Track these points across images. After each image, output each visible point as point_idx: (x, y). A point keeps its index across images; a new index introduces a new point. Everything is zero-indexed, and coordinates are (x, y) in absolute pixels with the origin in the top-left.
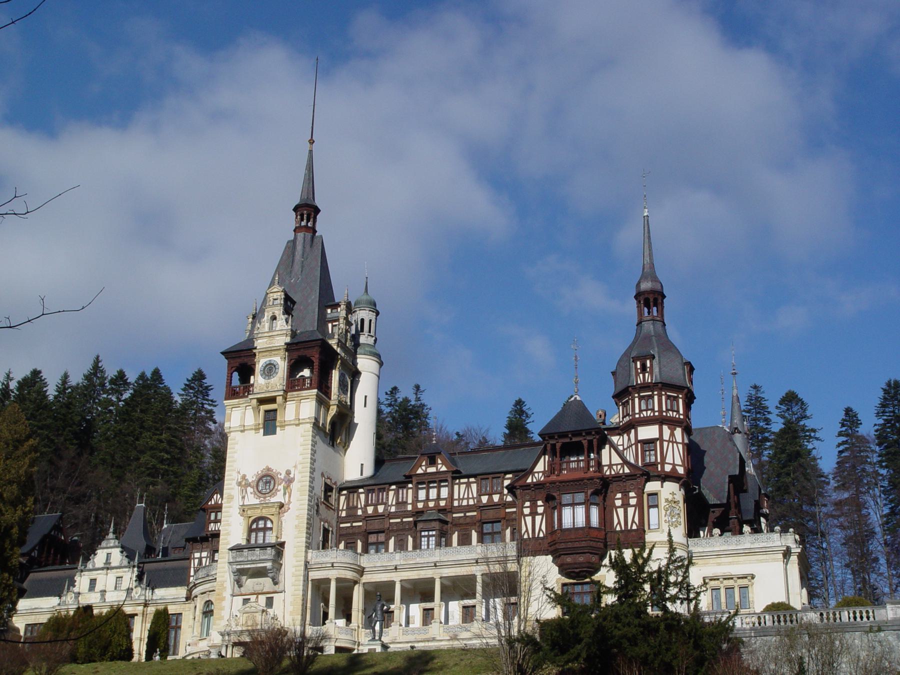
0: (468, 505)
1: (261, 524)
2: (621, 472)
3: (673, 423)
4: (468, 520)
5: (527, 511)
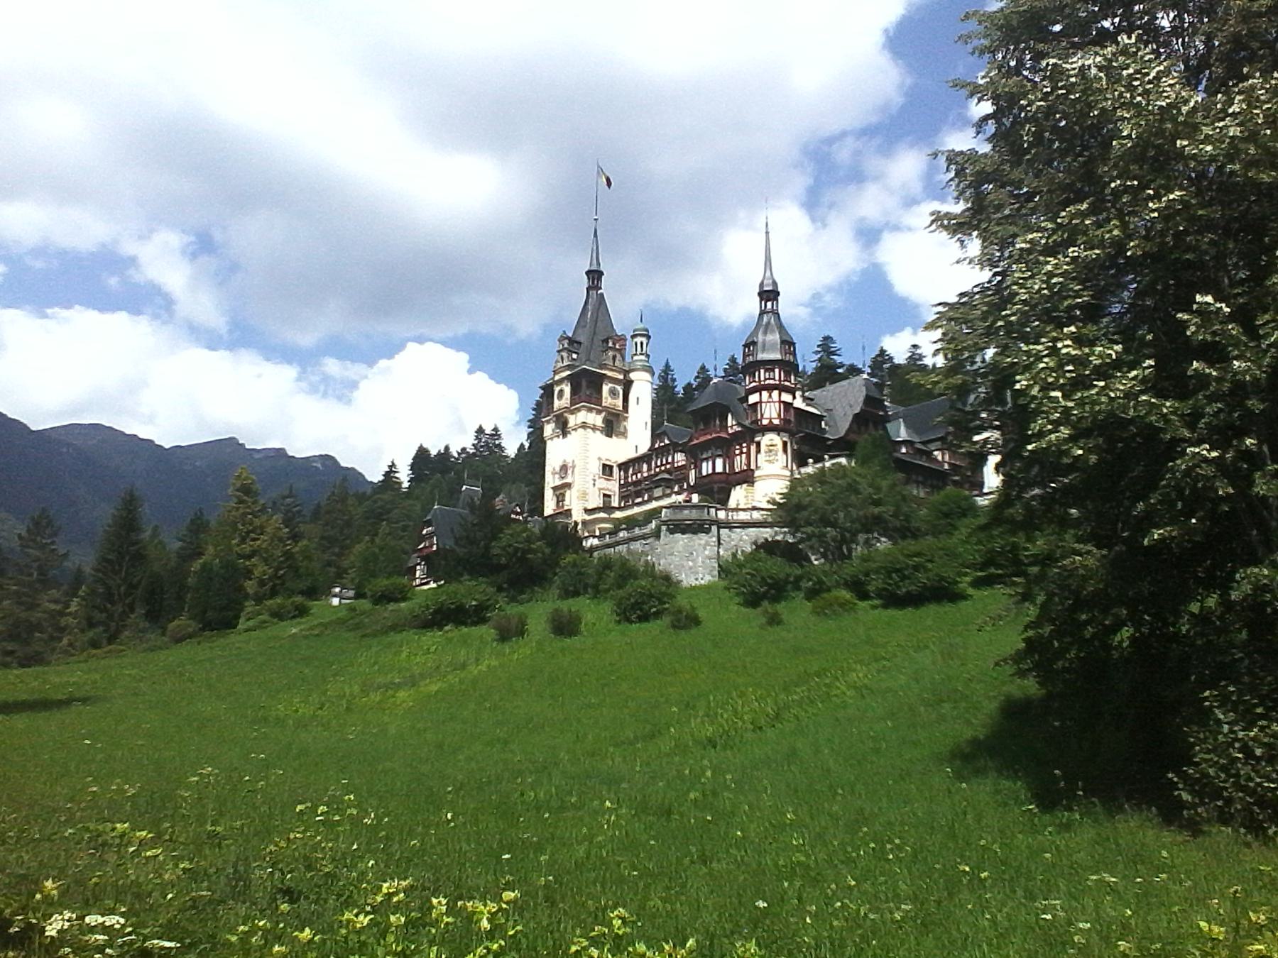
3: (770, 388)
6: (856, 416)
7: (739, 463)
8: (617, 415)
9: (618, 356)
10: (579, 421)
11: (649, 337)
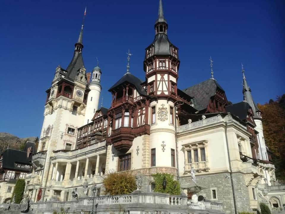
2: (140, 99)
3: (162, 72)
6: (212, 98)
8: (79, 105)
9: (84, 77)
11: (101, 72)
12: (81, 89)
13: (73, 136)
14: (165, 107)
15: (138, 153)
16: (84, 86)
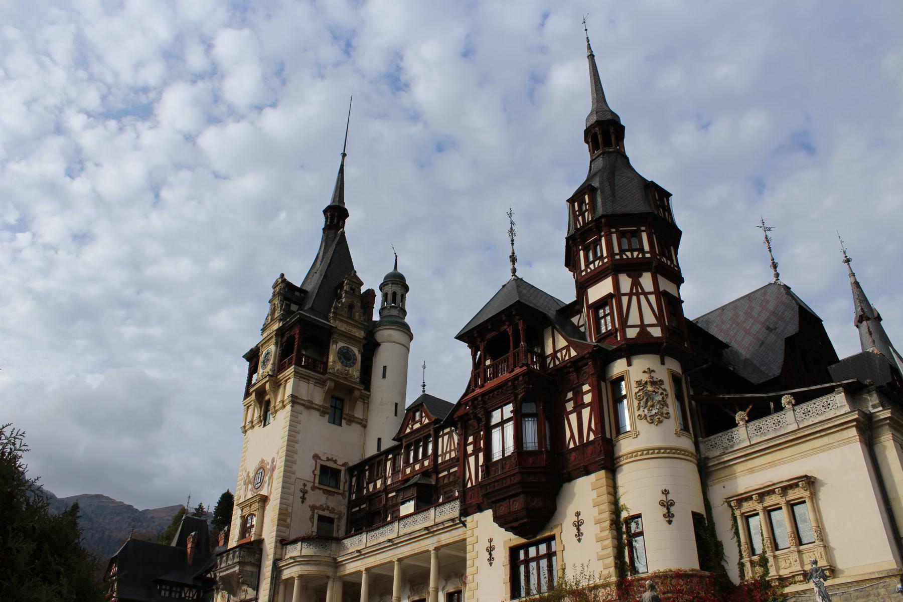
0: (451, 459)
1: (249, 525)
2: (567, 358)
3: (634, 269)
4: (452, 479)
5: (470, 449)
7: (579, 425)
8: (350, 391)
10: (286, 397)
12: (349, 343)
13: (338, 494)
14: (657, 376)
15: (579, 535)
16: (361, 334)
